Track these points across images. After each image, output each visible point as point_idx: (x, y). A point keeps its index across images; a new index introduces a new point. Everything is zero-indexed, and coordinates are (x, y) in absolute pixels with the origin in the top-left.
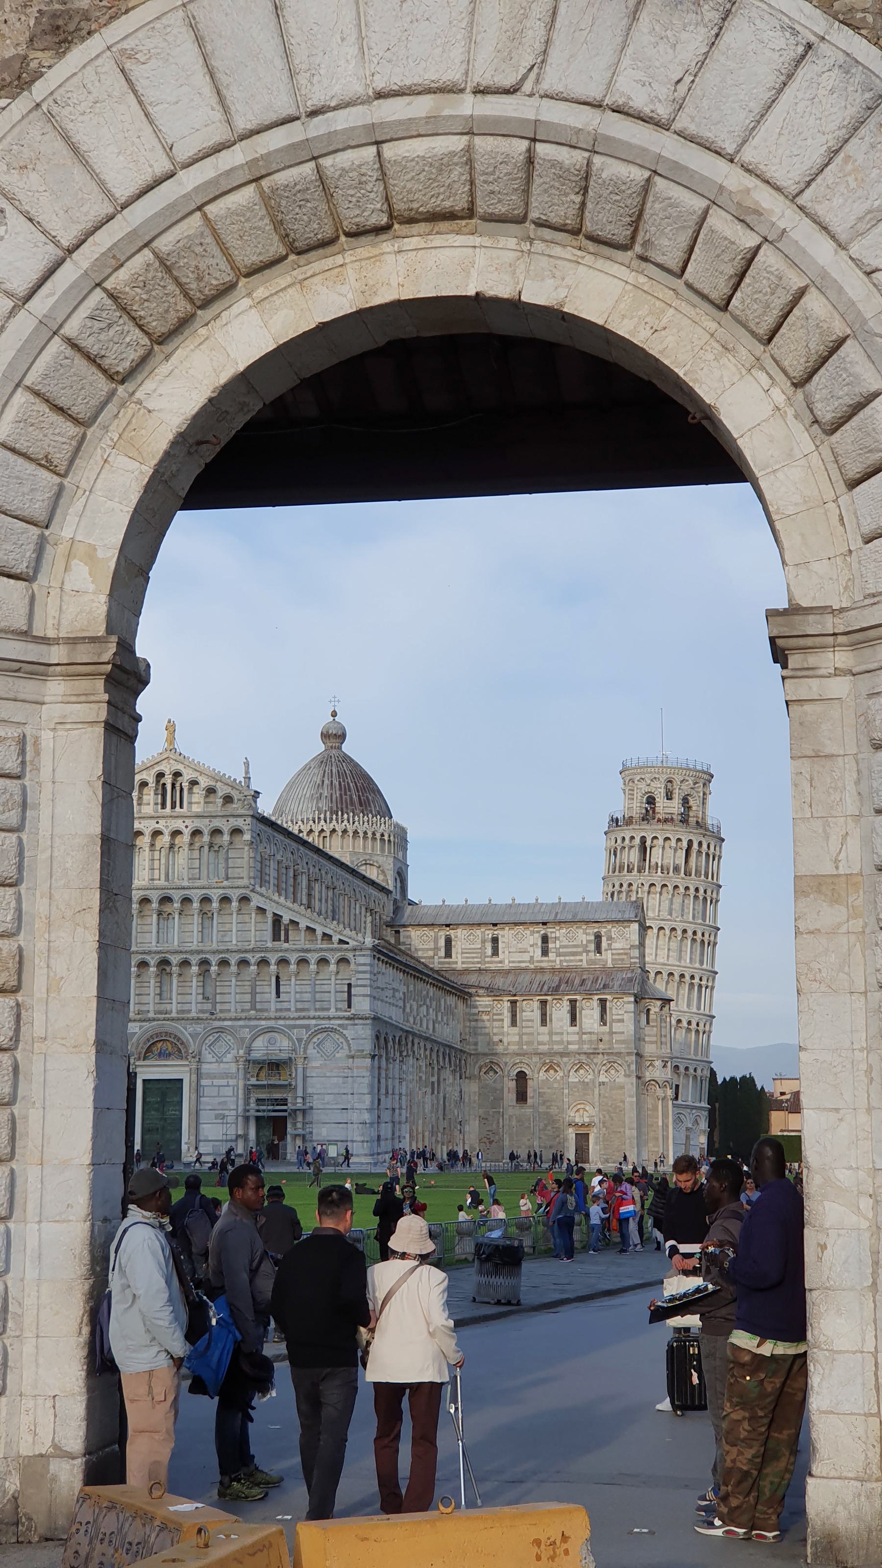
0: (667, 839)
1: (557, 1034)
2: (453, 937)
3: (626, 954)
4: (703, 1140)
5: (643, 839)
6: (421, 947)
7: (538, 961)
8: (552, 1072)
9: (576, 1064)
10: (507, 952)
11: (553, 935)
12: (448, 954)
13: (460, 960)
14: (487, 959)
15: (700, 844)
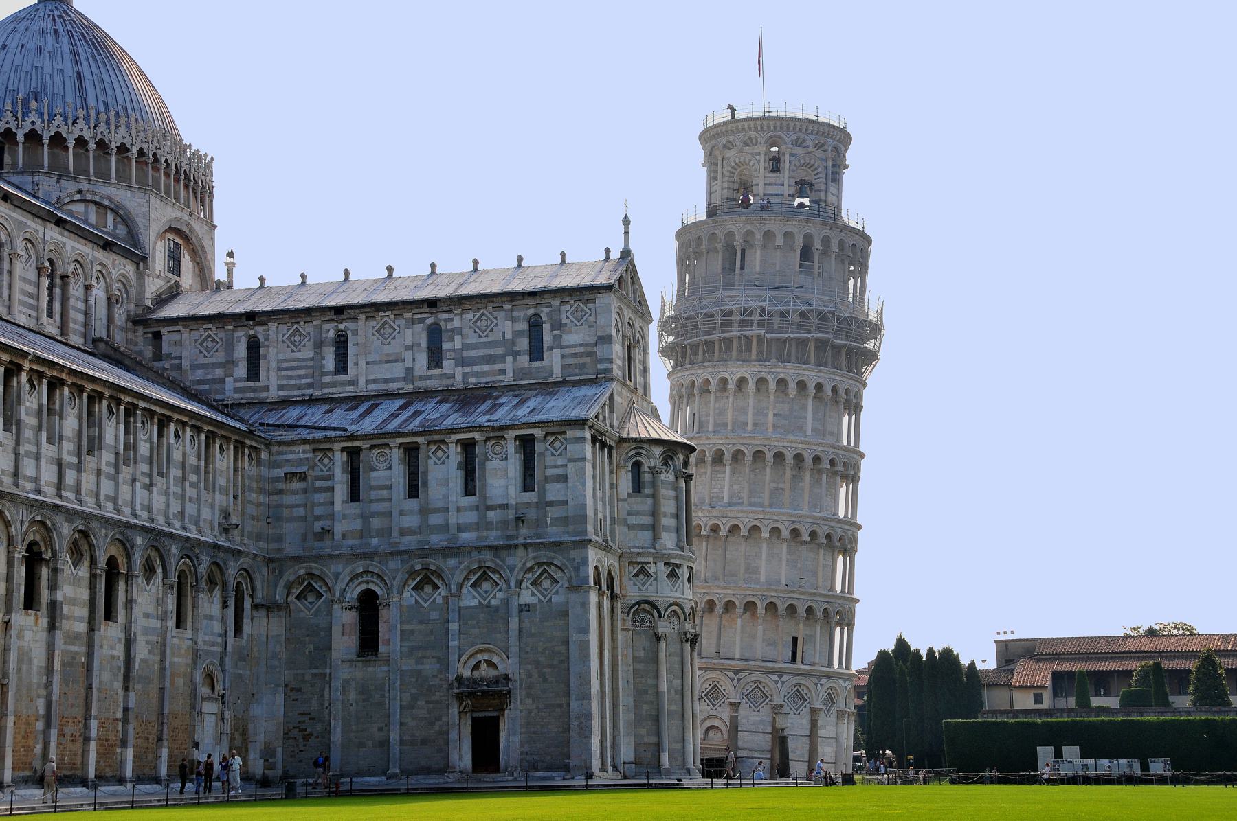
0: (768, 235)
1: (437, 511)
2: (262, 339)
3: (589, 354)
4: (847, 730)
5: (730, 234)
6: (206, 361)
7: (421, 378)
8: (428, 589)
9: (473, 572)
10: (362, 363)
11: (449, 326)
12: (253, 372)
13: (274, 383)
14: (326, 379)
15: (826, 241)
